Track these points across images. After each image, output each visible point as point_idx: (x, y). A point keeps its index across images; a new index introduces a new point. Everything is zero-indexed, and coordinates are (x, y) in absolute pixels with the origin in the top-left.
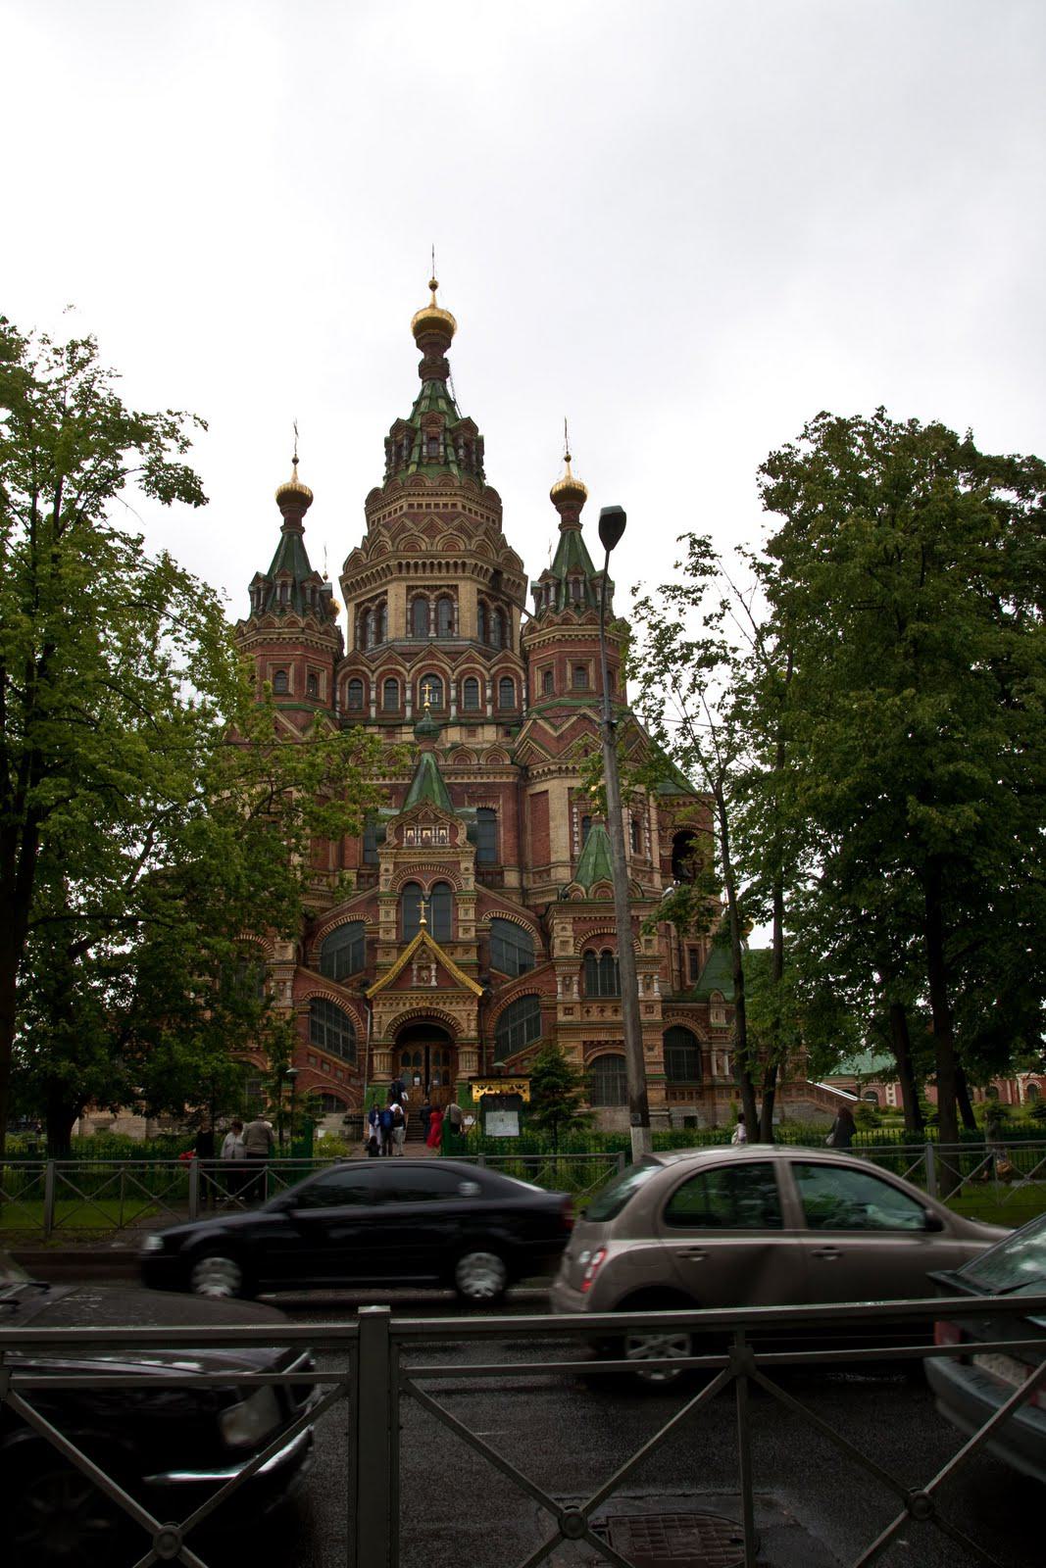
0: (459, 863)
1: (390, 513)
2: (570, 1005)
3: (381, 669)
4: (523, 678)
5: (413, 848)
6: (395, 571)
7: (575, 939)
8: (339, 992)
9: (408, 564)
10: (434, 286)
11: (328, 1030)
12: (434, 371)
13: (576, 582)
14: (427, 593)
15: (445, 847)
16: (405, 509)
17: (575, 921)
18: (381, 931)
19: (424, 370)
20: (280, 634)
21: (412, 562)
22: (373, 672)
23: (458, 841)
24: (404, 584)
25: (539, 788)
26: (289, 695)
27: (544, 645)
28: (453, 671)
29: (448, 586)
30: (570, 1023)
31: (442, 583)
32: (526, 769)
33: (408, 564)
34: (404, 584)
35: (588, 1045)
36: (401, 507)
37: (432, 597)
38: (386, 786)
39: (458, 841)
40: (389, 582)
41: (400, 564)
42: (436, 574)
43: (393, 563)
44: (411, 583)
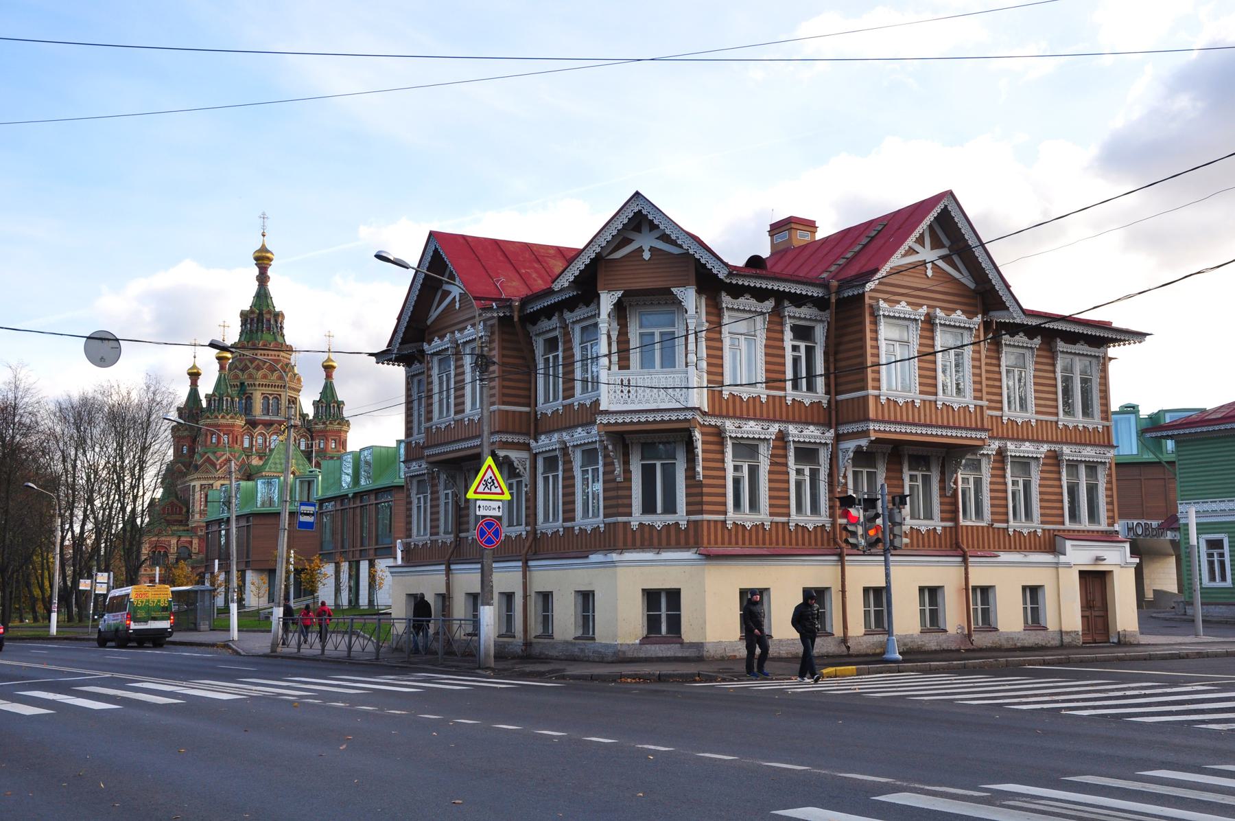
12: (263, 279)
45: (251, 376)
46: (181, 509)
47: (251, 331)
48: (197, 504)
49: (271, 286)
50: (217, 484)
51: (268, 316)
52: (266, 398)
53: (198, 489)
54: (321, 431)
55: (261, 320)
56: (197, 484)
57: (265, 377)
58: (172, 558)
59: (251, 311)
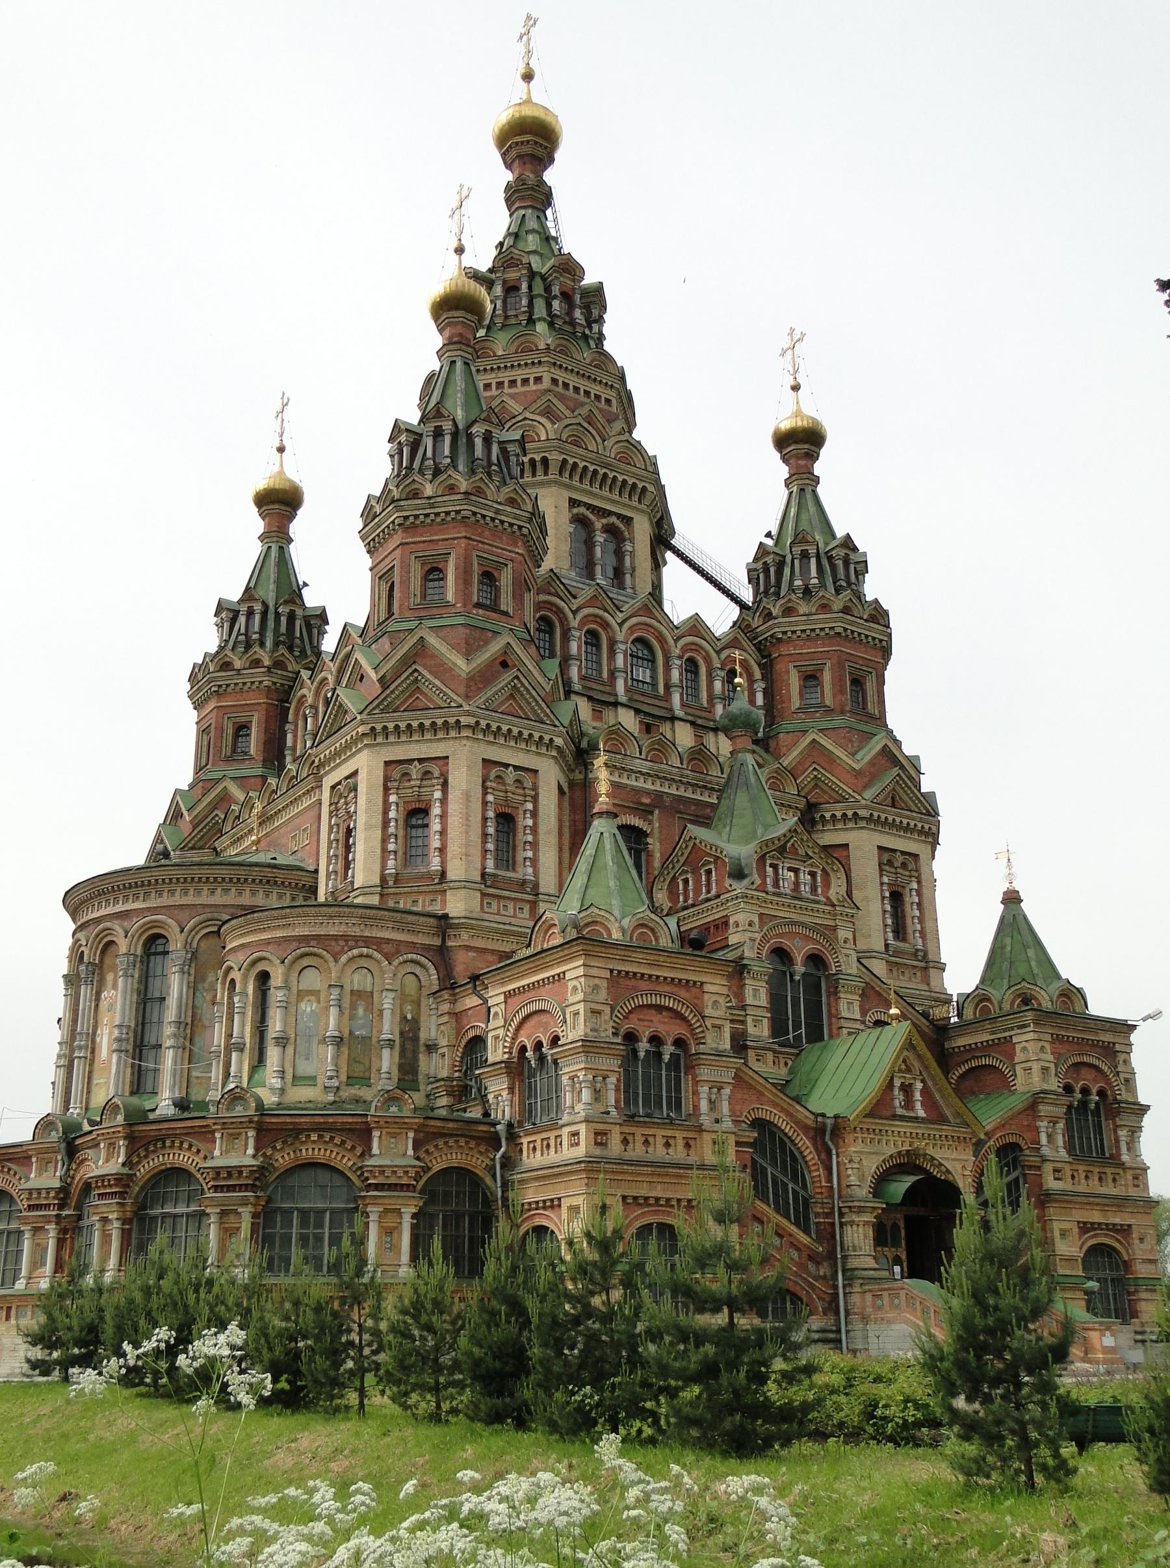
0: (834, 929)
1: (513, 383)
2: (1059, 1165)
3: (586, 611)
4: (758, 674)
5: (779, 895)
7: (1056, 1065)
8: (788, 1114)
10: (528, 77)
11: (774, 1177)
12: (530, 196)
14: (591, 517)
15: (818, 902)
16: (546, 383)
17: (1057, 1040)
18: (749, 1019)
20: (498, 512)
21: (582, 464)
22: (574, 613)
23: (832, 894)
24: (566, 494)
25: (829, 838)
26: (506, 614)
27: (811, 637)
28: (676, 641)
29: (619, 516)
30: (1064, 1193)
31: (613, 509)
32: (811, 807)
34: (566, 494)
35: (1085, 1228)
36: (538, 380)
37: (598, 525)
38: (648, 793)
39: (832, 894)
40: (542, 484)
41: (565, 461)
42: (605, 493)
44: (575, 496)
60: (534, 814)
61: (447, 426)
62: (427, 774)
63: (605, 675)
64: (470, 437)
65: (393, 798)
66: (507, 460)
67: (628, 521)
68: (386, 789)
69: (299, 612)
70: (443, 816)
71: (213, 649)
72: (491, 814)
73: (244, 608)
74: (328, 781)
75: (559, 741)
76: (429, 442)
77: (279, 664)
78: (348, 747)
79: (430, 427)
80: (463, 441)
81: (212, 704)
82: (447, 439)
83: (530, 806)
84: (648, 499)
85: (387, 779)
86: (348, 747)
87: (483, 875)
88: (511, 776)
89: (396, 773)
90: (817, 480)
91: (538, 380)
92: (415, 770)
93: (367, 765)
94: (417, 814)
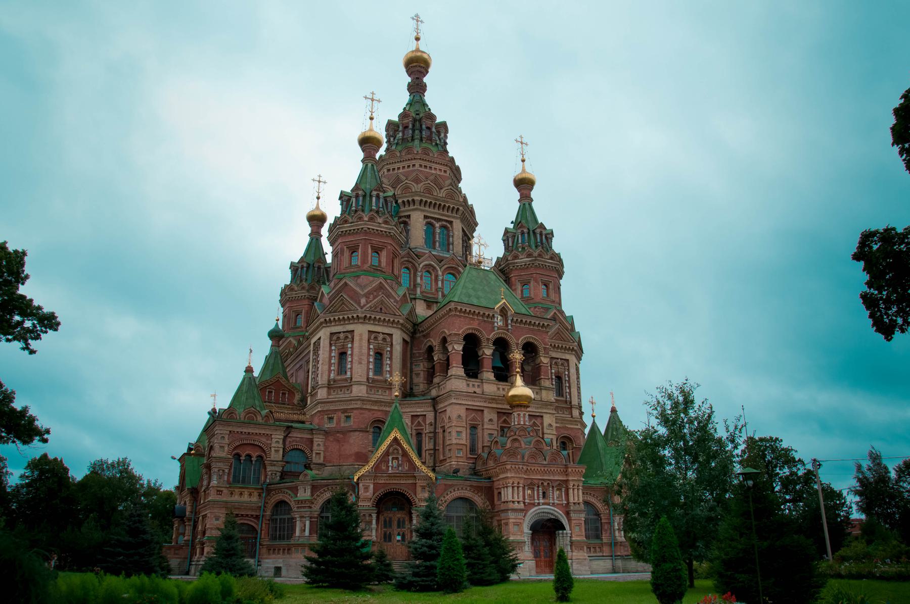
1: (404, 167)
6: (417, 203)
9: (426, 202)
10: (417, 39)
12: (417, 88)
13: (541, 234)
16: (417, 165)
19: (411, 88)
33: (426, 202)
36: (414, 165)
37: (437, 225)
40: (413, 210)
41: (421, 200)
43: (419, 198)
45: (407, 188)
46: (292, 394)
47: (403, 139)
48: (323, 367)
49: (429, 98)
50: (361, 330)
51: (429, 122)
52: (430, 225)
53: (325, 344)
54: (526, 267)
55: (418, 130)
56: (323, 334)
57: (428, 190)
58: (273, 471)
59: (403, 116)
60: (391, 352)
61: (360, 192)
62: (347, 337)
63: (434, 290)
64: (371, 196)
65: (333, 348)
66: (387, 204)
67: (451, 223)
68: (331, 345)
69: (322, 266)
70: (352, 355)
71: (288, 283)
72: (371, 353)
73: (300, 266)
74: (313, 341)
75: (401, 321)
76: (354, 200)
77: (312, 288)
78: (318, 327)
79: (354, 194)
80: (368, 198)
81: (287, 305)
82: (361, 198)
83: (389, 349)
84: (460, 212)
85: (331, 340)
86: (318, 327)
87: (368, 379)
88: (381, 337)
89: (335, 338)
90: (532, 200)
91: (414, 165)
92: (342, 335)
93: (323, 334)
94: (342, 355)
